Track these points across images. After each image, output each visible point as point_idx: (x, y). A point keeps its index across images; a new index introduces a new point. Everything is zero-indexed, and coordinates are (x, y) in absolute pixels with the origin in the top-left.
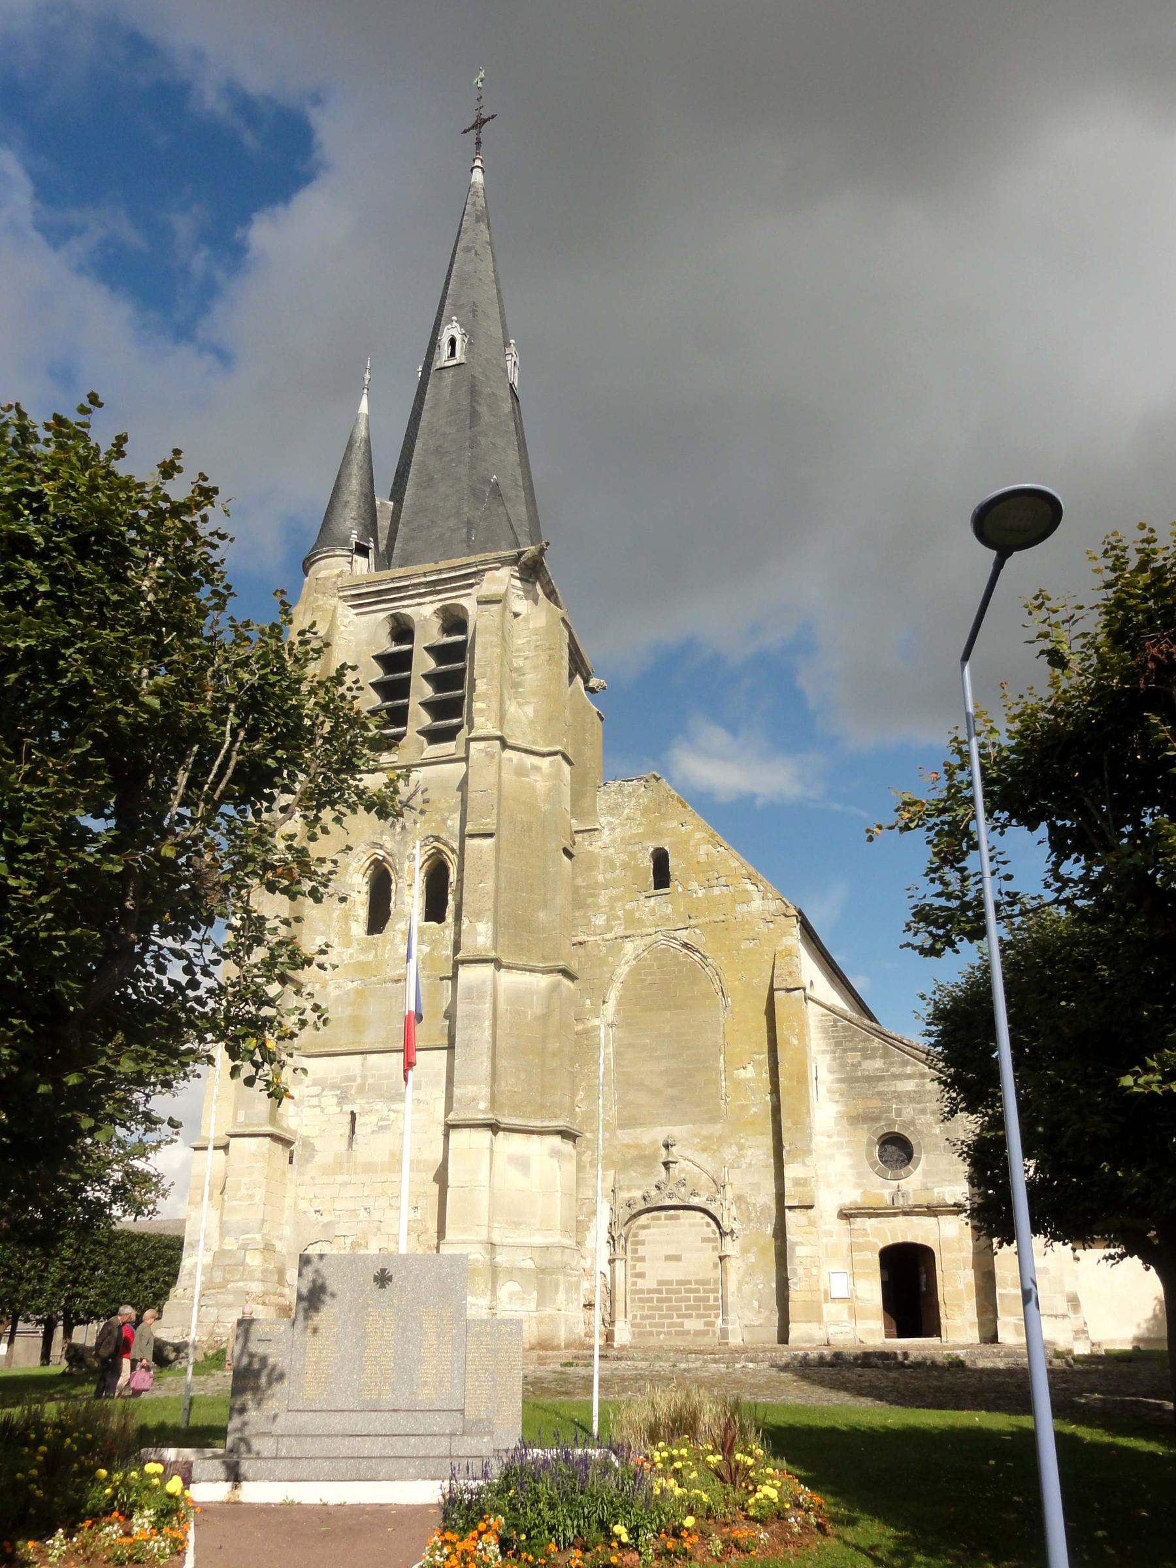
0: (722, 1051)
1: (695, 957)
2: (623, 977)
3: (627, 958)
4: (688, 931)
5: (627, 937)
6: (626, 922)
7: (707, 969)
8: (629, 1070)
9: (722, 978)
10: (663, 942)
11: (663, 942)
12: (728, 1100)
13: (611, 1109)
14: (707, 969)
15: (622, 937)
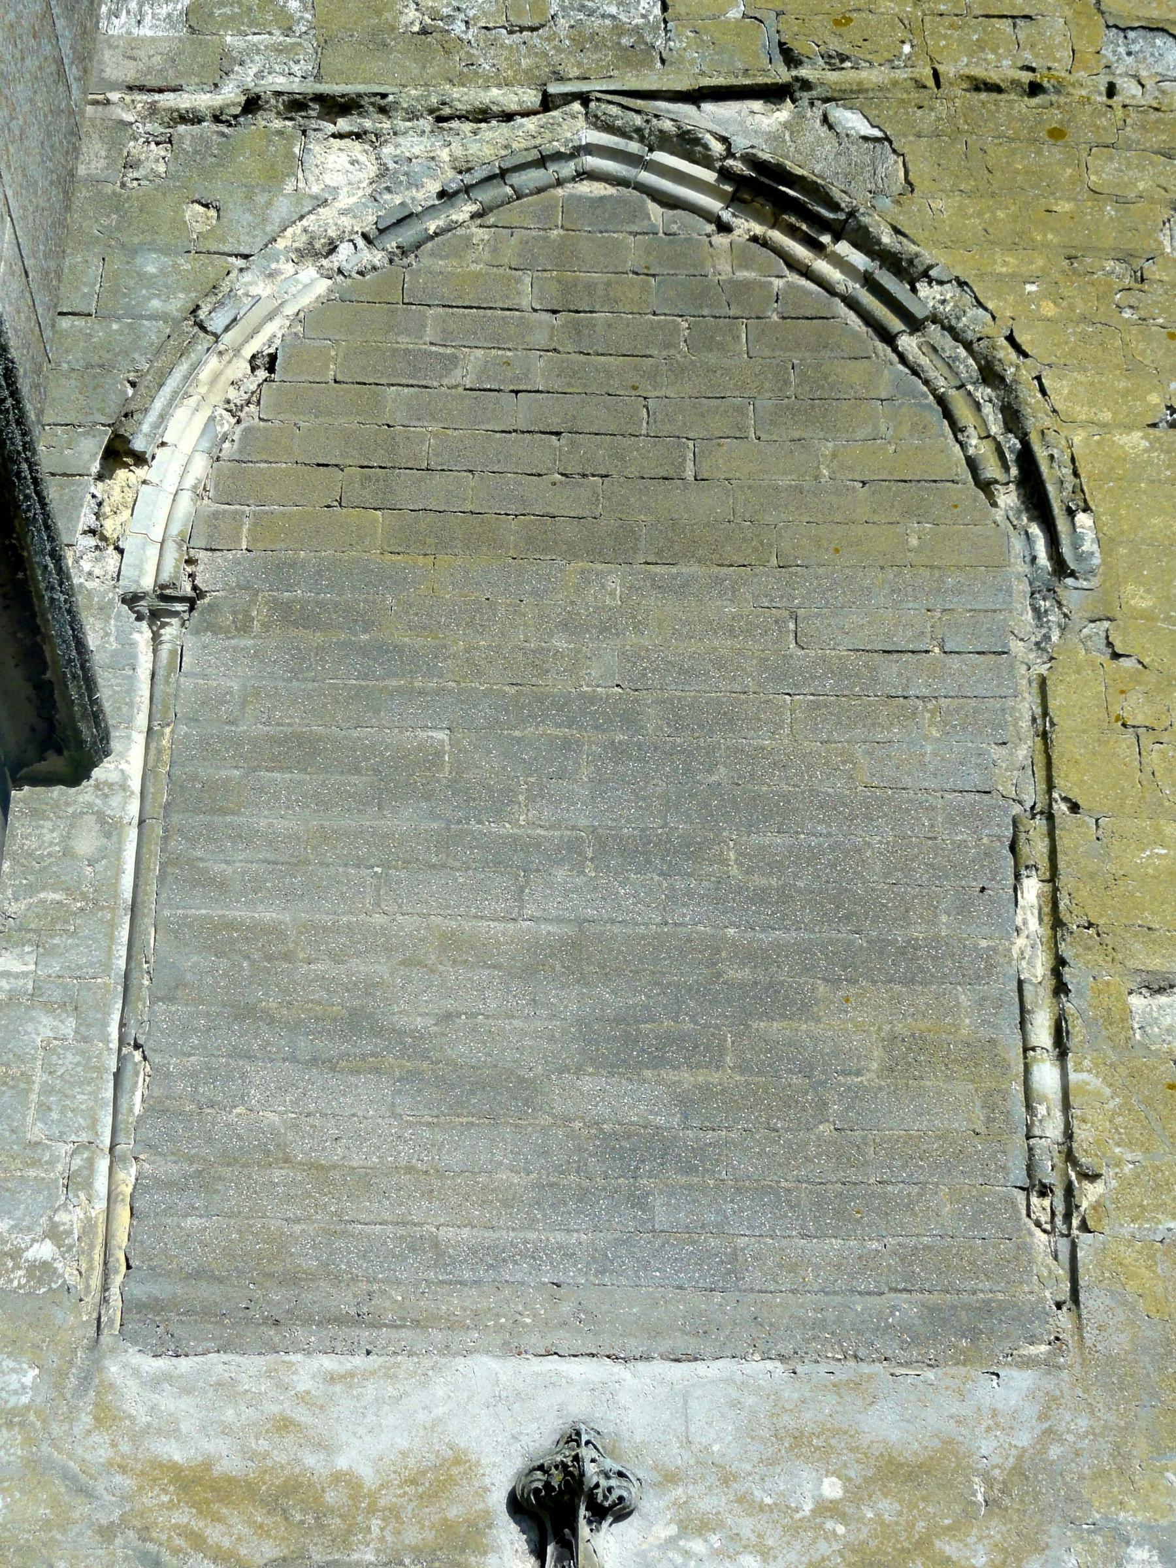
0: (1036, 848)
1: (822, 266)
2: (274, 328)
3: (327, 221)
4: (784, 113)
5: (335, 107)
6: (325, 43)
7: (908, 343)
8: (267, 915)
9: (1030, 396)
10: (592, 162)
11: (592, 162)
12: (1090, 1194)
13: (77, 1181)
14: (908, 343)
15: (296, 105)
